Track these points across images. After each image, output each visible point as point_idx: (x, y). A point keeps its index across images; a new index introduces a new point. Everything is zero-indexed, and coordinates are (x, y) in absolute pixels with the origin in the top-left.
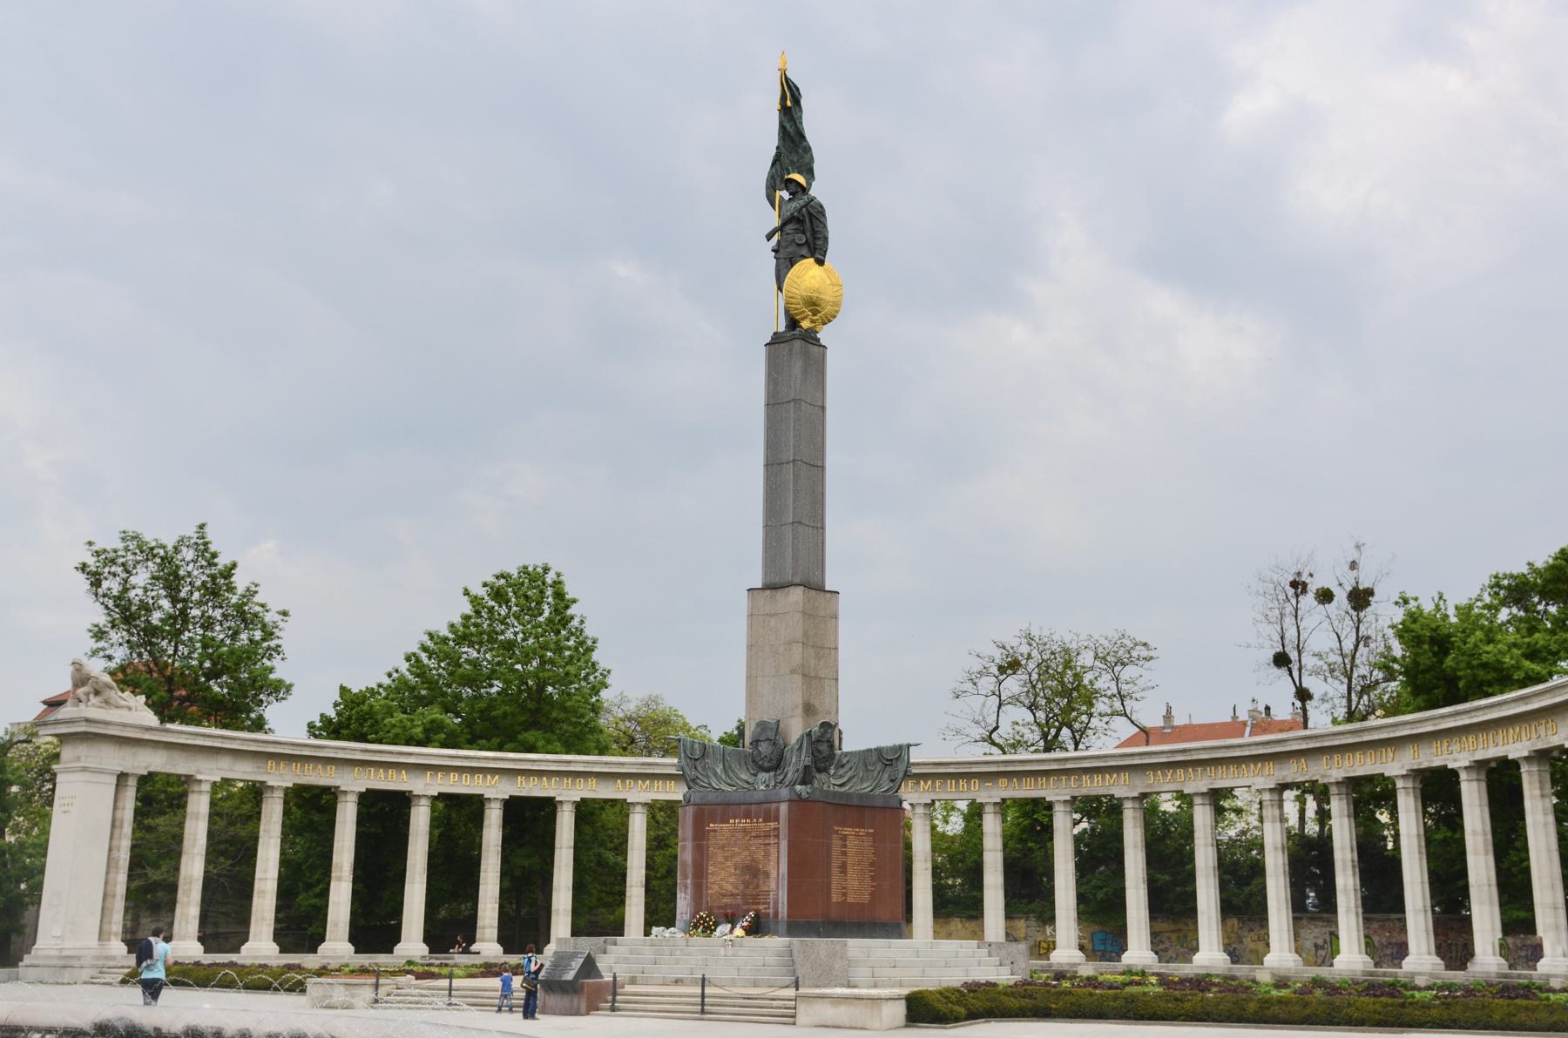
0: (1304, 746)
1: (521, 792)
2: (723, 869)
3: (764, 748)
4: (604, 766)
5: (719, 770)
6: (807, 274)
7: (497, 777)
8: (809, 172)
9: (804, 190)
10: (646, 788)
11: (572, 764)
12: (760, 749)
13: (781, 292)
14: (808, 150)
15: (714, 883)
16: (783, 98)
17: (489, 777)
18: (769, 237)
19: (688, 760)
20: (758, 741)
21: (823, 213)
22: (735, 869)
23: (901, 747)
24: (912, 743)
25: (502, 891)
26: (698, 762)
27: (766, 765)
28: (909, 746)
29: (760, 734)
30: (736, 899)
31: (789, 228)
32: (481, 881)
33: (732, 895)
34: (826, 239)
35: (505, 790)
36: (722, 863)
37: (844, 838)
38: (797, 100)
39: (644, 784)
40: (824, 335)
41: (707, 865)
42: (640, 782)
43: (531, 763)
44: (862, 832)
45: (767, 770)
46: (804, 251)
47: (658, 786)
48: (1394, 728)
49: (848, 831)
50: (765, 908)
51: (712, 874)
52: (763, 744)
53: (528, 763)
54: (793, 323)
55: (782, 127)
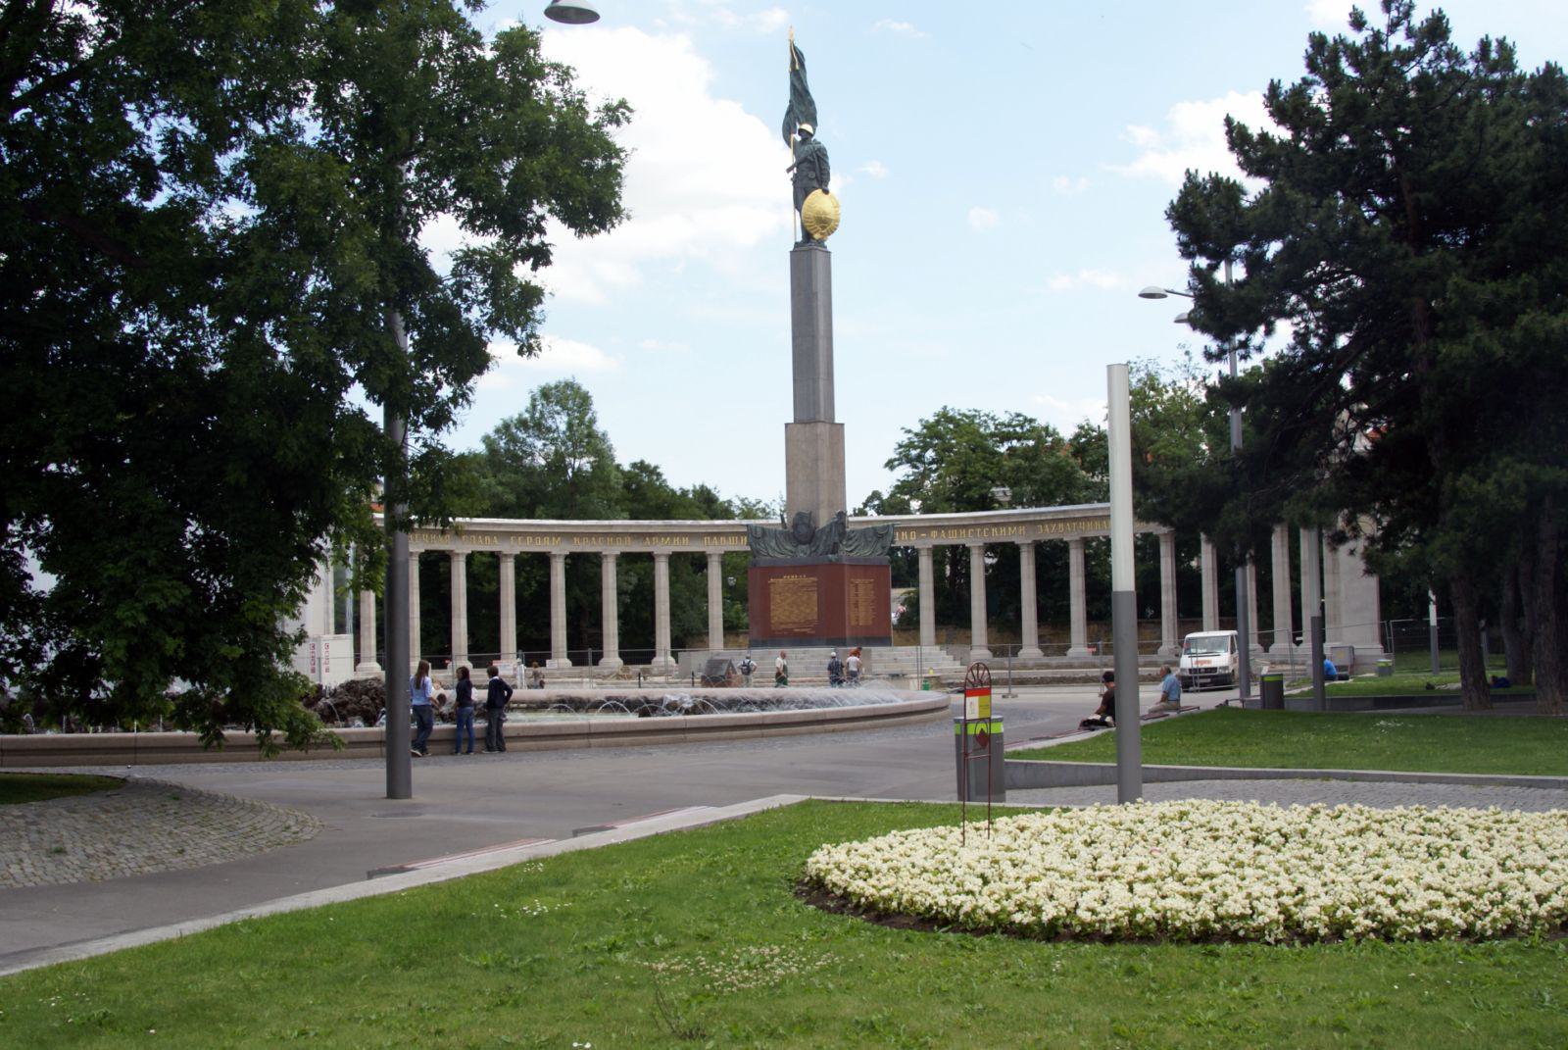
5: (773, 544)
6: (816, 200)
8: (813, 121)
9: (812, 135)
13: (800, 211)
14: (812, 103)
16: (793, 63)
18: (789, 170)
21: (826, 155)
31: (805, 165)
34: (828, 174)
37: (856, 586)
38: (802, 65)
40: (830, 243)
44: (867, 581)
45: (804, 544)
46: (815, 184)
49: (858, 581)
54: (808, 236)
55: (793, 87)
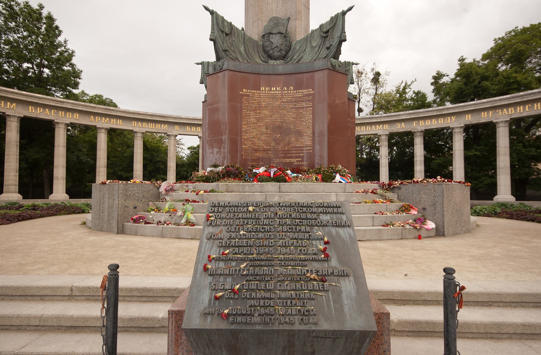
0: (409, 117)
1: (31, 114)
2: (255, 128)
3: (276, 40)
4: (84, 107)
5: (242, 49)
7: (14, 104)
10: (107, 121)
11: (65, 104)
12: (272, 40)
15: (247, 139)
17: (9, 103)
19: (220, 32)
20: (271, 33)
22: (267, 129)
23: (349, 63)
24: (354, 62)
25: (21, 169)
26: (228, 38)
27: (276, 54)
28: (353, 64)
29: (273, 28)
30: (268, 154)
32: (6, 160)
33: (264, 150)
35: (21, 112)
36: (256, 123)
39: (106, 119)
41: (241, 125)
42: (103, 118)
43: (38, 99)
45: (276, 59)
47: (113, 122)
48: (463, 107)
50: (298, 161)
51: (246, 131)
52: (274, 36)
53: (35, 99)
